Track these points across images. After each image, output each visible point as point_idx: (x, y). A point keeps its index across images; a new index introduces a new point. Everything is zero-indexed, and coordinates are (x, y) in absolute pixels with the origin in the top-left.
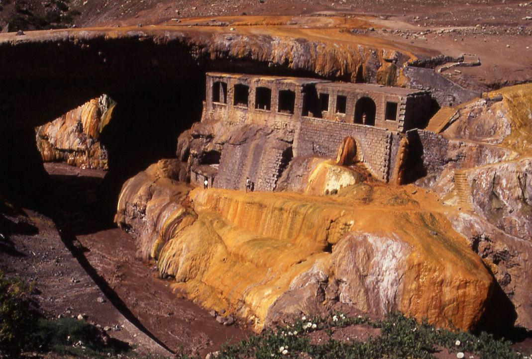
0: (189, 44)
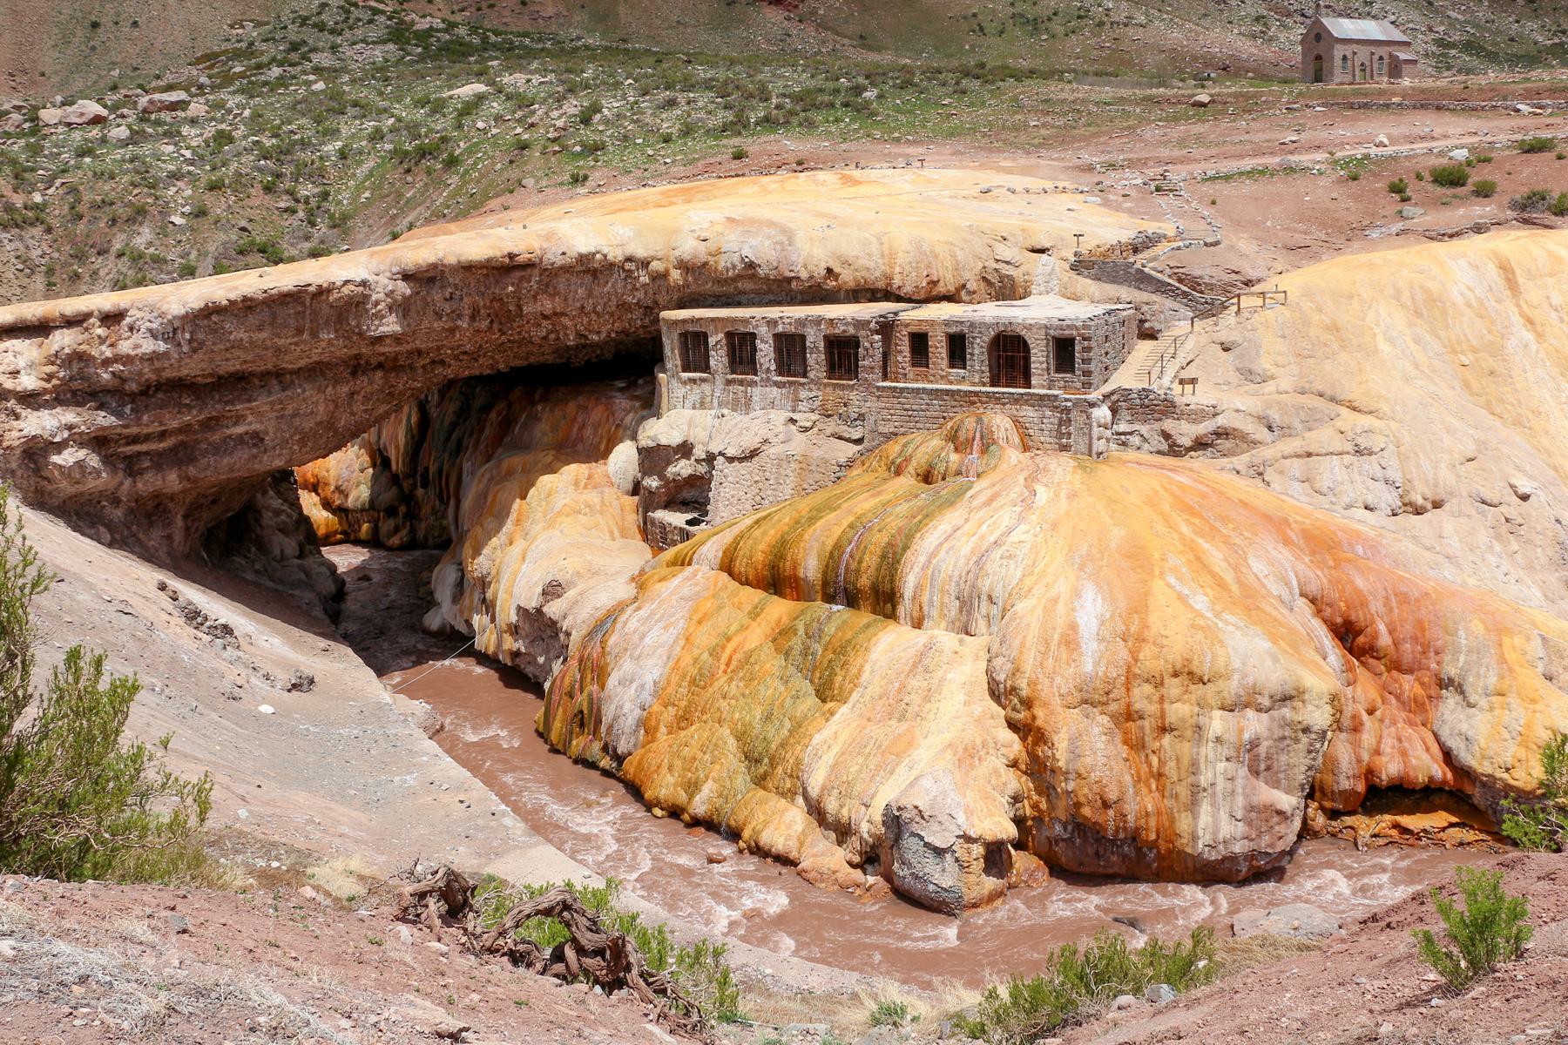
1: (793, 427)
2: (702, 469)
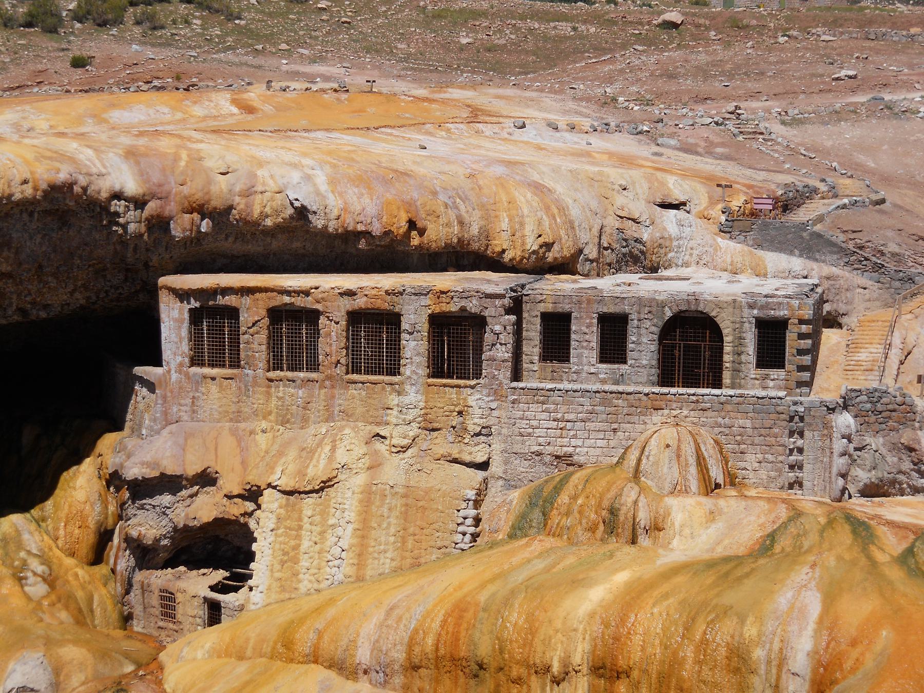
0: (104, 195)
1: (380, 446)
2: (235, 509)
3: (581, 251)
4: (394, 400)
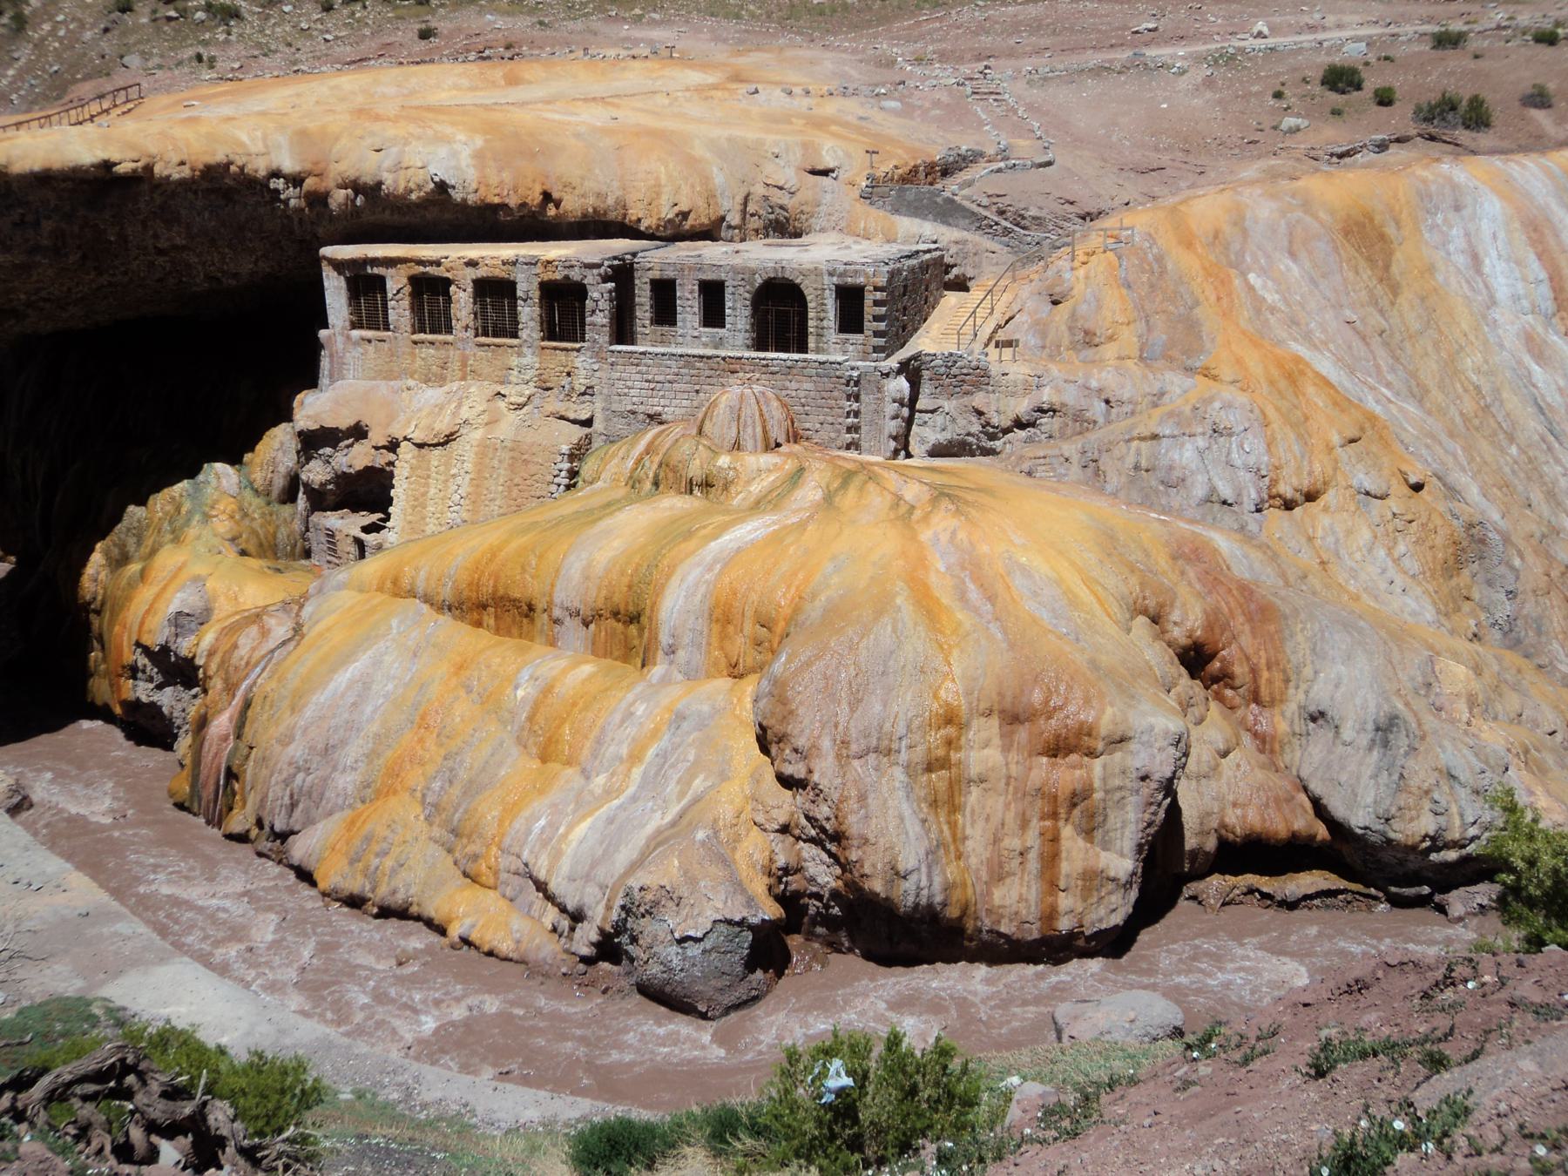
0: (262, 173)
2: (381, 459)
3: (723, 219)
4: (514, 361)
